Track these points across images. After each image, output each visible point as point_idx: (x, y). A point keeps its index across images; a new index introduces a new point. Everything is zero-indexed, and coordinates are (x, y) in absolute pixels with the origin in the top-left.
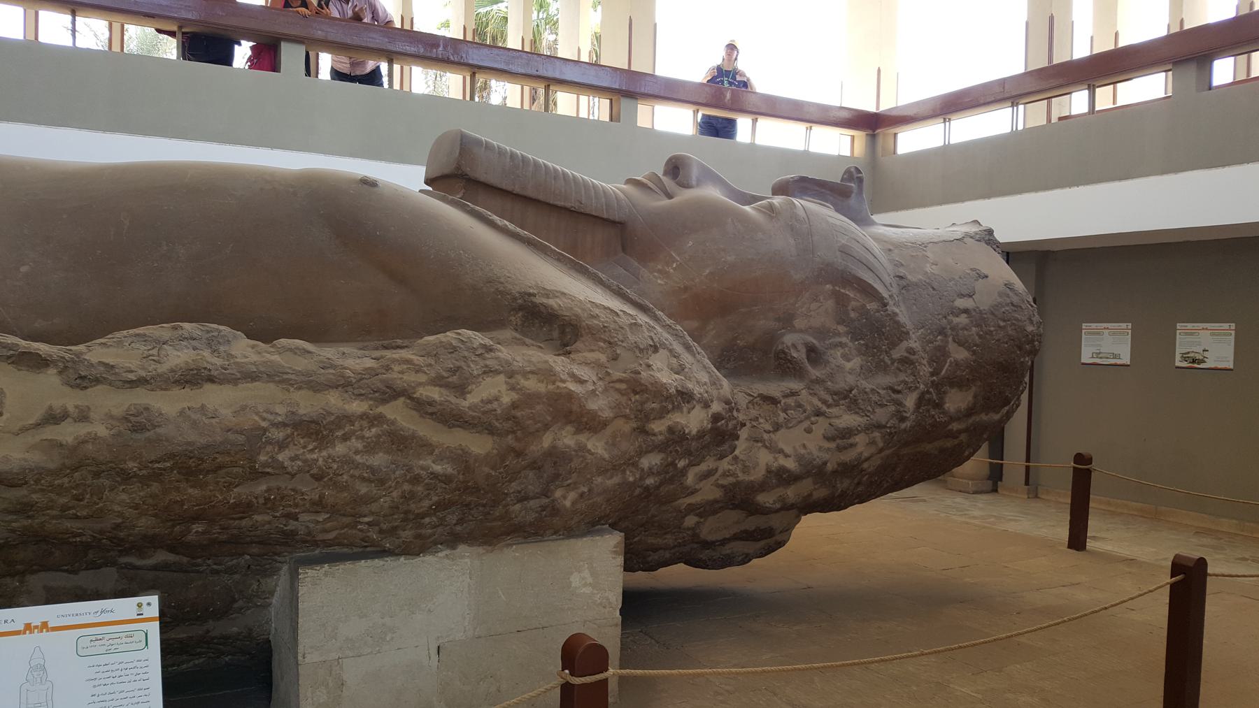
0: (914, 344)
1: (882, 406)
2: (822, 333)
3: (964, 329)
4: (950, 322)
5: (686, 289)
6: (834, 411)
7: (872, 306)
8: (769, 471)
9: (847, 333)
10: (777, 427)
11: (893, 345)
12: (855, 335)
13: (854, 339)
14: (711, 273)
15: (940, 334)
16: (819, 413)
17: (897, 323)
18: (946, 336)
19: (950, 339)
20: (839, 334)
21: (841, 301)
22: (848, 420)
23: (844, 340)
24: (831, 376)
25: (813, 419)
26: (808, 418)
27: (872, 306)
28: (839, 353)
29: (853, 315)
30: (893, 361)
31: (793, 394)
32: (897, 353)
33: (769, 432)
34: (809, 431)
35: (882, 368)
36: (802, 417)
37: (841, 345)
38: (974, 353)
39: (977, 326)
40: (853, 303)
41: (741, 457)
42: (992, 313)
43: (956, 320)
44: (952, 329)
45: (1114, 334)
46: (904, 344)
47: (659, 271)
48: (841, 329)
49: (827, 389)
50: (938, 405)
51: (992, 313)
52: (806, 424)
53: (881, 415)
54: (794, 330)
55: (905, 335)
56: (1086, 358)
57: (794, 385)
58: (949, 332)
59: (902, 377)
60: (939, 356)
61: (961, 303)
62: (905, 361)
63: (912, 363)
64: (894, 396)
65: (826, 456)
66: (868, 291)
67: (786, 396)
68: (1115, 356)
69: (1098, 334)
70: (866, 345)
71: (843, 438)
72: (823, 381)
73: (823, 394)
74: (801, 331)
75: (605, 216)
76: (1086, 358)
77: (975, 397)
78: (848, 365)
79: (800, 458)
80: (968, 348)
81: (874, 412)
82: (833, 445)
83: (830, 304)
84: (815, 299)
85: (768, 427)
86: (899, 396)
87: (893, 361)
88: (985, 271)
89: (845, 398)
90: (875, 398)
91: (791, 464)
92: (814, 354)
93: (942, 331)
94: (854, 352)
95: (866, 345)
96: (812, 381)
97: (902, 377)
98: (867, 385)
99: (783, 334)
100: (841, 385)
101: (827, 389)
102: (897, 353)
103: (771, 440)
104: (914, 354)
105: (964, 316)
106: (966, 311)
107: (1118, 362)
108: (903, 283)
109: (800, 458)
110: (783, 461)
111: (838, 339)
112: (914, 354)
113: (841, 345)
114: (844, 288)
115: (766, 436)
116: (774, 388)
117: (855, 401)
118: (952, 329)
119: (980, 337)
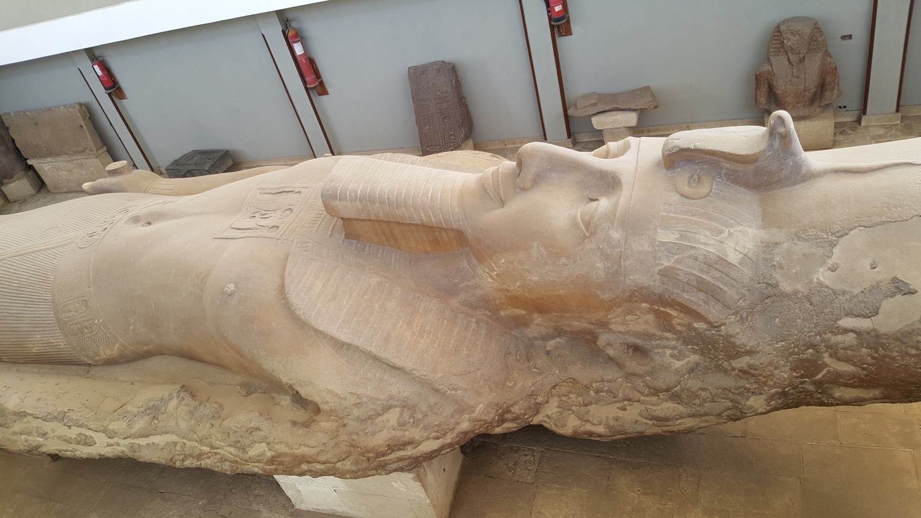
1: (713, 401)
5: (507, 291)
7: (700, 326)
24: (650, 373)
27: (700, 326)
28: (668, 352)
30: (733, 369)
52: (620, 405)
57: (611, 373)
64: (731, 395)
72: (640, 376)
78: (678, 364)
80: (854, 364)
82: (651, 423)
83: (650, 318)
84: (631, 312)
91: (601, 429)
98: (693, 384)
105: (852, 335)
109: (607, 426)
110: (589, 427)
119: (873, 358)
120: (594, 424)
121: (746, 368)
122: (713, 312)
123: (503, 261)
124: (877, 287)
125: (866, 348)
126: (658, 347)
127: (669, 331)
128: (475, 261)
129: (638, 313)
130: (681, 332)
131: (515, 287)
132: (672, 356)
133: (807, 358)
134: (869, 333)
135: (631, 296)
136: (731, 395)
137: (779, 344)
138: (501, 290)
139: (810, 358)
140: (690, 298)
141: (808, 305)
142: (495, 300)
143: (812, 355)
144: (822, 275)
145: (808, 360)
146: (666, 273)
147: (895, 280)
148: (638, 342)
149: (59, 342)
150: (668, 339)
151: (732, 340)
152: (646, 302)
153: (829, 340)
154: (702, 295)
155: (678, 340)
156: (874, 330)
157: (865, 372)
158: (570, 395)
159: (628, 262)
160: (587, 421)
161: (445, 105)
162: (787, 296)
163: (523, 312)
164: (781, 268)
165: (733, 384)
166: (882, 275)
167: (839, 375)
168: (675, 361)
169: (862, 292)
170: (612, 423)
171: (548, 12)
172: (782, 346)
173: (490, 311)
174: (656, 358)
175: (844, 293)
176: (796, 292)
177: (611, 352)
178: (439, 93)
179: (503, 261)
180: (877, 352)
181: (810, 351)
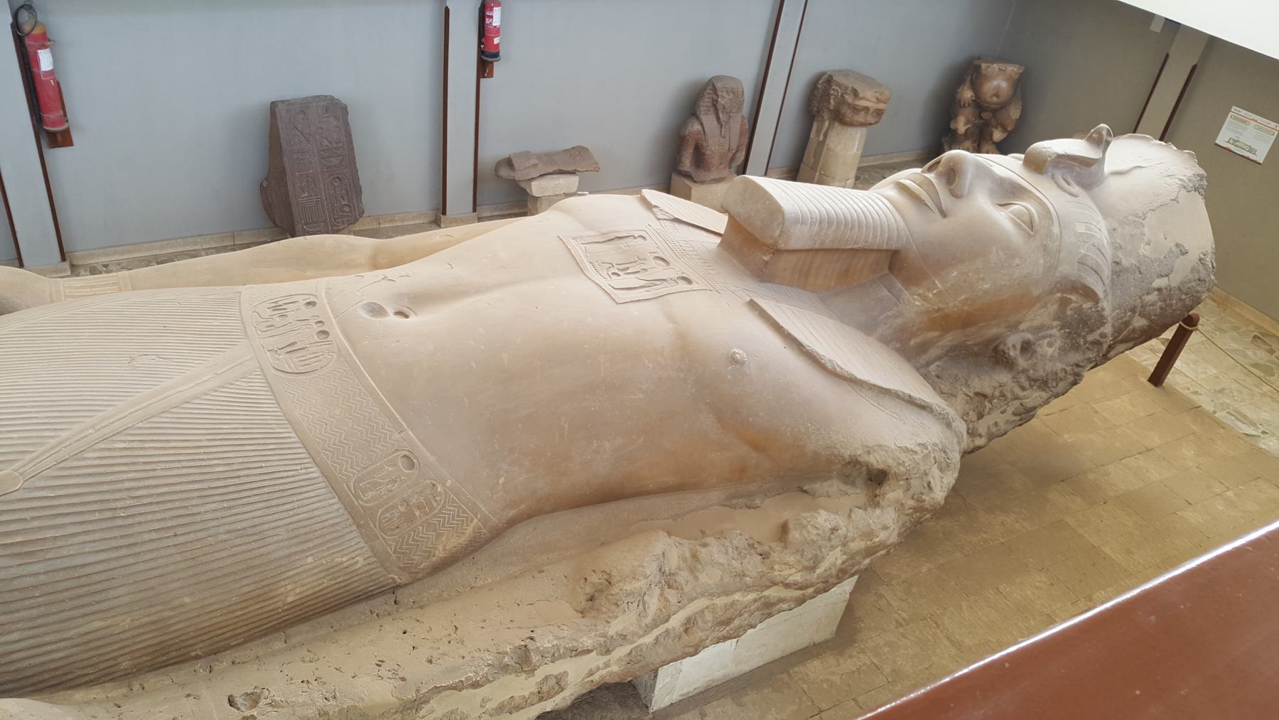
3: (1152, 305)
4: (1142, 301)
5: (939, 310)
11: (1092, 331)
21: (1064, 303)
23: (1054, 331)
29: (1069, 313)
32: (1094, 336)
35: (1075, 347)
40: (1073, 305)
42: (1180, 289)
45: (1259, 129)
47: (919, 295)
48: (1055, 323)
55: (1103, 324)
56: (1222, 140)
57: (1004, 377)
61: (1158, 283)
64: (1077, 370)
66: (1089, 294)
68: (1251, 150)
69: (1245, 122)
73: (1023, 379)
76: (1222, 140)
82: (1017, 418)
87: (1086, 342)
92: (1026, 347)
107: (1252, 157)
111: (1050, 332)
113: (1051, 336)
119: (1161, 308)
124: (1171, 251)
126: (1044, 337)
128: (899, 285)
131: (954, 304)
132: (1050, 345)
136: (1077, 370)
138: (928, 312)
144: (1144, 250)
147: (1177, 245)
148: (1029, 336)
149: (355, 557)
161: (335, 161)
163: (936, 334)
166: (1170, 244)
167: (1134, 330)
171: (480, 43)
174: (1039, 350)
178: (326, 142)
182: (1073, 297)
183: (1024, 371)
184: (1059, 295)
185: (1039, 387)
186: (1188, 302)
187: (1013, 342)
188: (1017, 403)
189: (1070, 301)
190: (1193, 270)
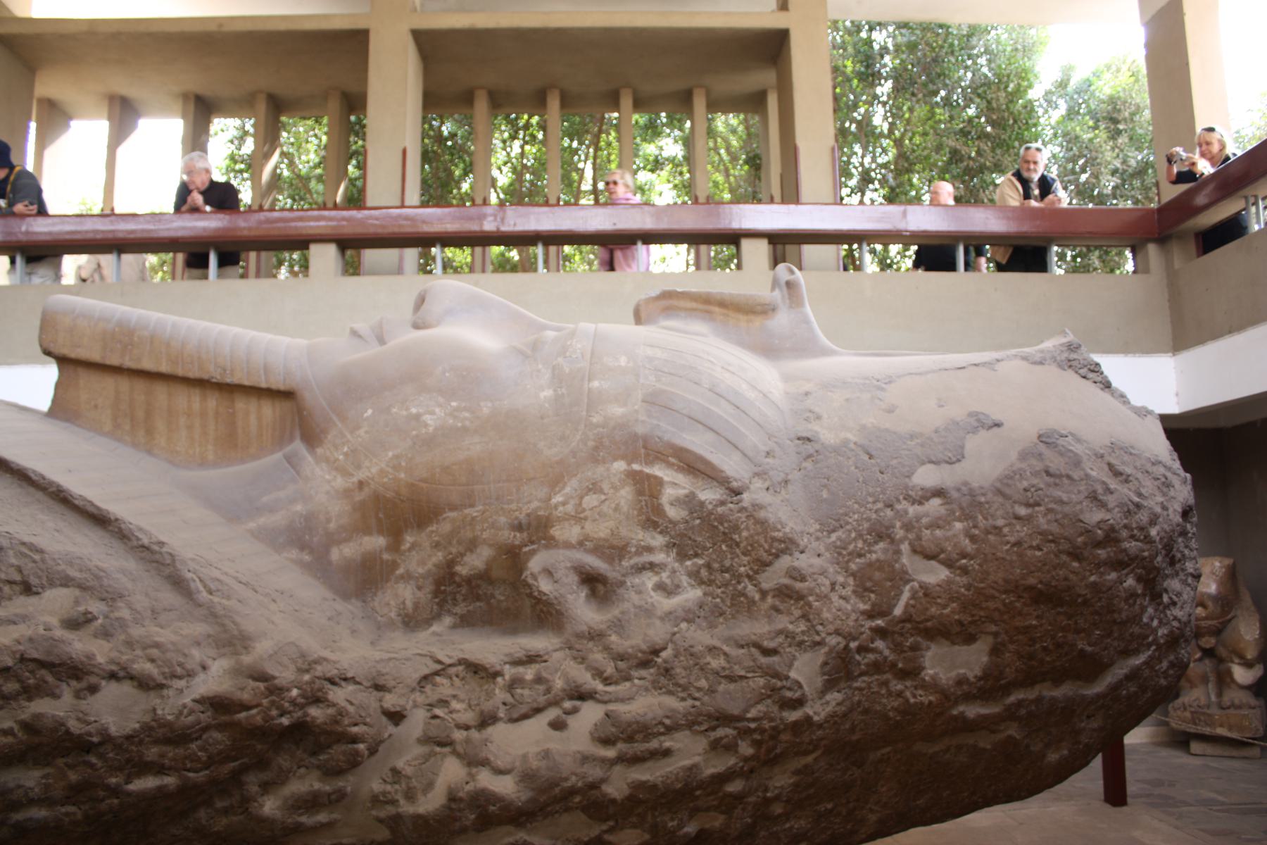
0: (803, 562)
1: (731, 679)
2: (614, 550)
3: (934, 525)
4: (901, 515)
5: (361, 484)
6: (623, 688)
8: (452, 798)
9: (669, 546)
10: (486, 720)
12: (682, 547)
13: (682, 556)
14: (397, 457)
15: (880, 537)
16: (582, 695)
17: (763, 523)
18: (892, 541)
19: (905, 547)
20: (649, 549)
22: (644, 703)
23: (659, 557)
24: (619, 625)
25: (568, 704)
26: (555, 703)
27: (709, 495)
28: (649, 580)
29: (672, 513)
30: (764, 594)
31: (531, 659)
32: (773, 577)
33: (467, 728)
34: (558, 725)
35: (741, 605)
36: (542, 700)
37: (652, 566)
38: (965, 571)
39: (965, 517)
41: (409, 771)
43: (913, 510)
44: (908, 527)
46: (785, 562)
47: (327, 461)
48: (658, 540)
49: (607, 648)
50: (911, 673)
51: (999, 492)
52: (552, 713)
53: (730, 698)
54: (551, 543)
58: (899, 533)
59: (783, 622)
60: (876, 582)
61: (926, 477)
62: (784, 593)
63: (800, 597)
64: (764, 660)
65: (595, 773)
66: (693, 466)
67: (517, 663)
70: (708, 566)
71: (630, 739)
73: (598, 657)
74: (568, 545)
75: (264, 385)
77: (995, 651)
78: (667, 604)
79: (527, 777)
80: (949, 564)
81: (711, 691)
82: (611, 753)
83: (626, 494)
84: (594, 488)
85: (468, 717)
86: (775, 659)
87: (764, 594)
88: (997, 417)
89: (644, 664)
90: (716, 663)
93: (881, 533)
94: (685, 580)
95: (708, 566)
96: (579, 636)
97: (783, 622)
98: (700, 637)
99: (533, 552)
100: (634, 641)
101: (607, 648)
102: (773, 577)
103: (468, 741)
104: (803, 579)
105: (936, 502)
106: (939, 493)
108: (809, 448)
109: (527, 777)
110: (485, 780)
111: (647, 558)
112: (803, 579)
113: (652, 566)
114: (649, 463)
115: (459, 735)
116: (490, 648)
117: (667, 671)
118: (908, 527)
119: (973, 539)
120: (500, 772)
121: (786, 581)
122: (731, 465)
123: (370, 412)
125: (960, 520)
127: (655, 525)
129: (605, 486)
130: (675, 523)
132: (660, 587)
133: (878, 560)
134: (959, 490)
135: (596, 448)
137: (834, 537)
138: (347, 493)
139: (882, 557)
140: (698, 443)
141: (866, 457)
142: (328, 521)
143: (885, 551)
145: (879, 565)
146: (654, 401)
148: (596, 563)
150: (649, 549)
151: (762, 514)
152: (623, 457)
153: (906, 512)
154: (710, 436)
155: (669, 546)
156: (966, 484)
157: (964, 580)
158: (455, 705)
159: (596, 384)
160: (484, 763)
162: (836, 450)
164: (819, 418)
165: (766, 628)
168: (663, 600)
169: (936, 431)
170: (535, 764)
172: (839, 539)
173: (312, 551)
175: (912, 437)
176: (845, 442)
177: (545, 586)
179: (370, 412)
180: (974, 518)
181: (881, 545)
182: (658, 471)
183: (595, 636)
184: (620, 466)
185: (656, 686)
186: (1042, 522)
187: (552, 572)
188: (591, 714)
189: (660, 482)
190: (1024, 456)
